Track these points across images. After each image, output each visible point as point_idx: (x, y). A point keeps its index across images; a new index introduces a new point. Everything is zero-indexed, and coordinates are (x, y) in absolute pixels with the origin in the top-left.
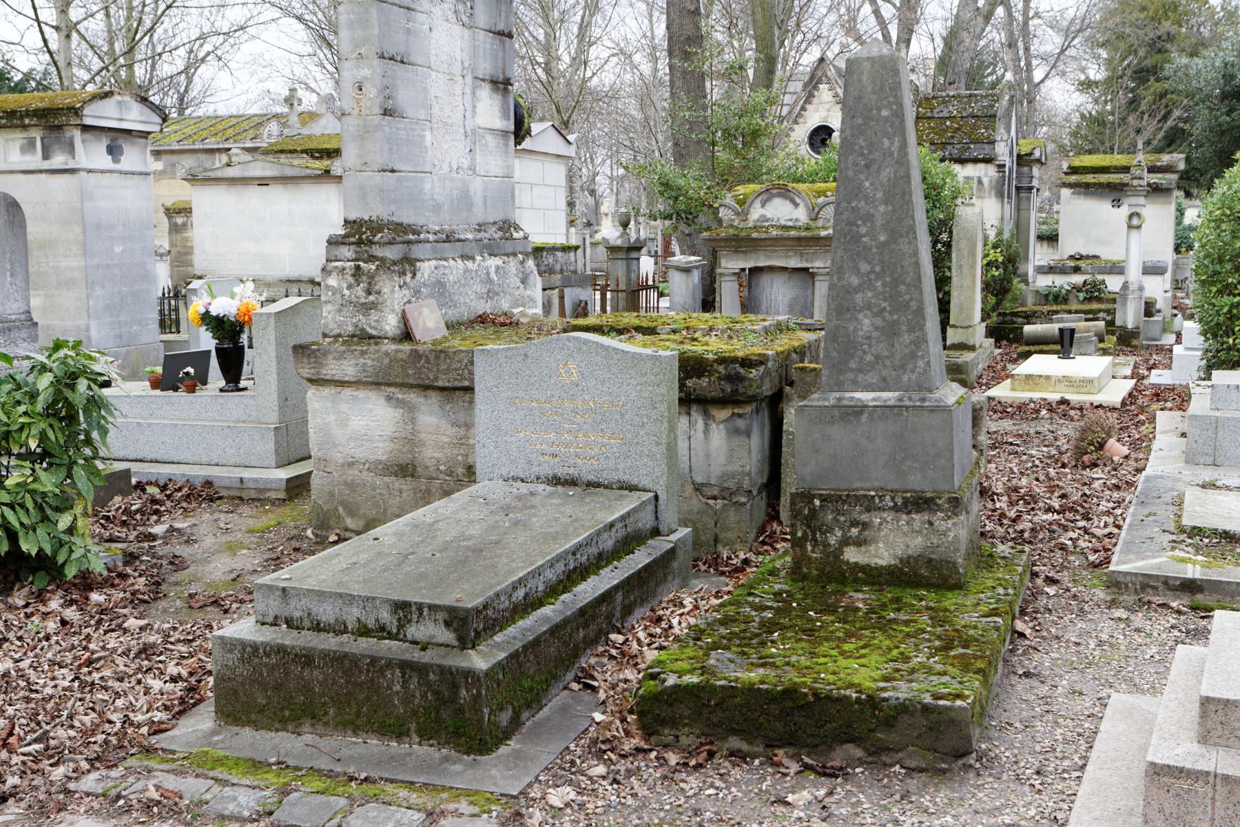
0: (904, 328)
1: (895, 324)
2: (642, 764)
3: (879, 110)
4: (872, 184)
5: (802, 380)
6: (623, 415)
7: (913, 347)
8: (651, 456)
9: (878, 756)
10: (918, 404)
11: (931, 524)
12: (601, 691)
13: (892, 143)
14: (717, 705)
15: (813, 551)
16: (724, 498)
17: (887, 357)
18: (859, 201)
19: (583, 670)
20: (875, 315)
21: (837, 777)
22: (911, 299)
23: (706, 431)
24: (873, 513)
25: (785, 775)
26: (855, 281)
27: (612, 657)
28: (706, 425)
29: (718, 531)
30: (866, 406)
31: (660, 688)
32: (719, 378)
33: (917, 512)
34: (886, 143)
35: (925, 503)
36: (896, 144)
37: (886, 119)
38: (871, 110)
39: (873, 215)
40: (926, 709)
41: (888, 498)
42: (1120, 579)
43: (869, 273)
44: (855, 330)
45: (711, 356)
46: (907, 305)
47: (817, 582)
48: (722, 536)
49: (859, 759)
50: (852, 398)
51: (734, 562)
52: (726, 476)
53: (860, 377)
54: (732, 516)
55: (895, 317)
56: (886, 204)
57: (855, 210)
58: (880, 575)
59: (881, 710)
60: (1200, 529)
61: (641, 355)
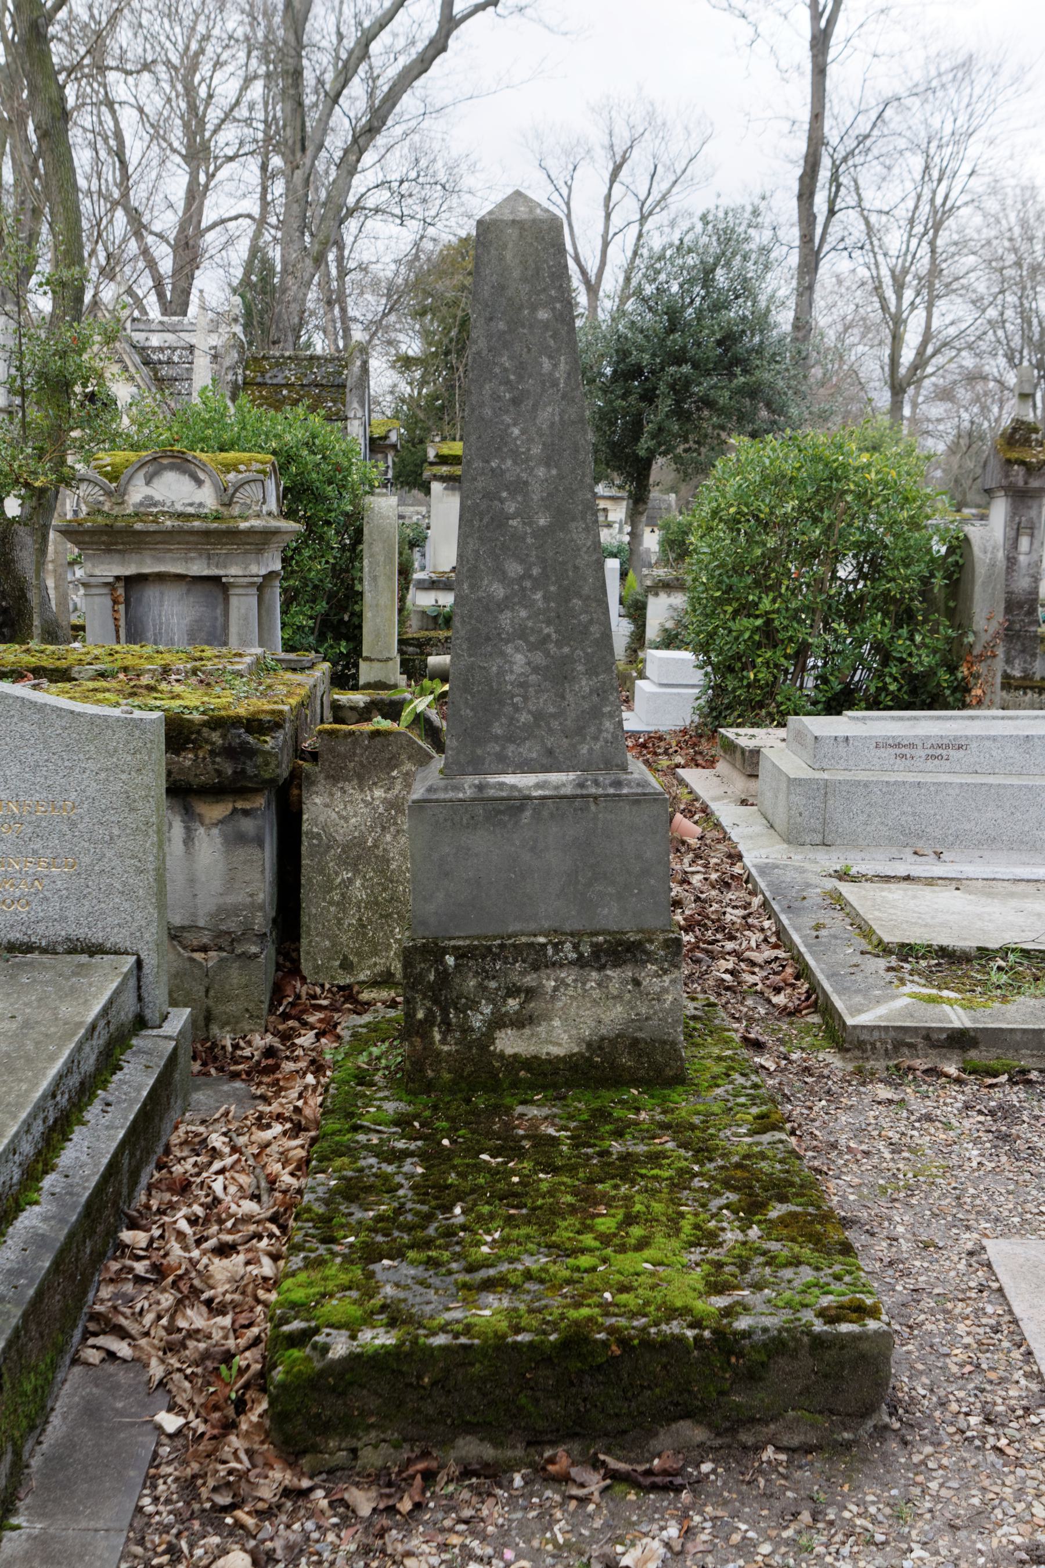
0: (580, 668)
1: (566, 661)
2: (310, 1525)
3: (534, 309)
4: (523, 432)
5: (331, 750)
6: (73, 825)
7: (595, 698)
8: (127, 893)
9: (734, 1435)
10: (611, 791)
11: (637, 983)
12: (154, 1362)
13: (555, 366)
14: (434, 1384)
15: (443, 1041)
16: (221, 949)
17: (553, 716)
18: (503, 460)
19: (95, 1317)
20: (532, 647)
21: (678, 1490)
22: (591, 621)
23: (189, 840)
24: (544, 973)
25: (583, 1501)
26: (499, 591)
27: (139, 1280)
28: (188, 830)
29: (210, 1003)
30: (529, 798)
31: (318, 1365)
32: (212, 752)
33: (615, 966)
34: (546, 364)
35: (628, 950)
36: (562, 366)
37: (546, 325)
38: (521, 308)
39: (526, 483)
40: (819, 1342)
41: (568, 946)
42: (865, 1036)
43: (522, 578)
44: (501, 673)
45: (196, 716)
46: (585, 632)
47: (452, 1092)
48: (218, 1010)
49: (701, 1445)
50: (502, 785)
51: (247, 1052)
52: (223, 912)
53: (511, 749)
54: (235, 976)
55: (566, 650)
56: (548, 465)
57: (497, 474)
58: (556, 1072)
59: (740, 1355)
60: (911, 947)
61: (106, 718)
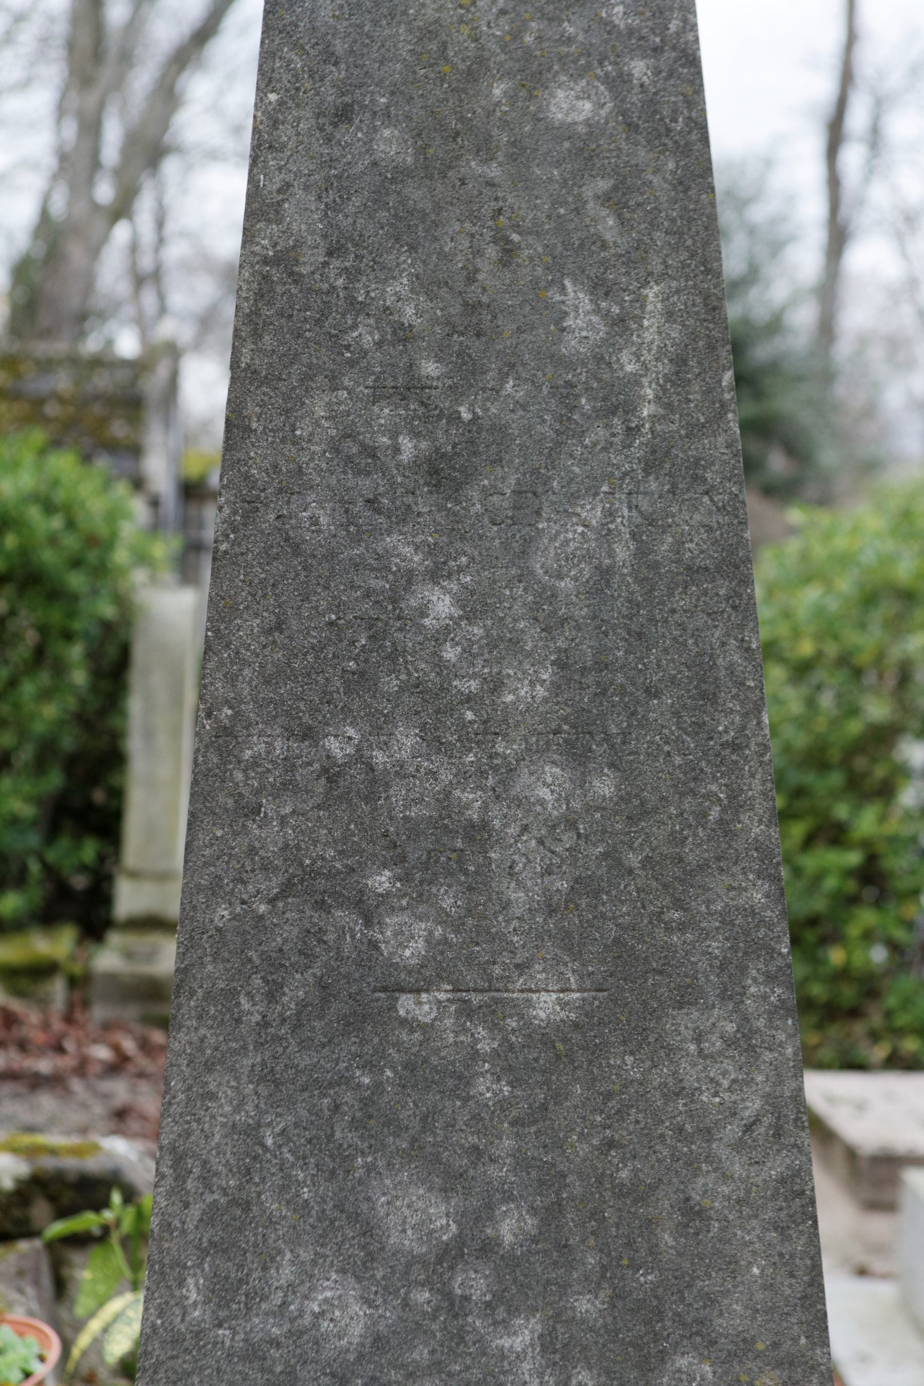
3: (533, 78)
4: (472, 607)
13: (621, 325)
18: (380, 727)
34: (582, 317)
36: (651, 328)
37: (584, 150)
38: (476, 71)
43: (450, 1255)
56: (577, 756)
57: (350, 788)
